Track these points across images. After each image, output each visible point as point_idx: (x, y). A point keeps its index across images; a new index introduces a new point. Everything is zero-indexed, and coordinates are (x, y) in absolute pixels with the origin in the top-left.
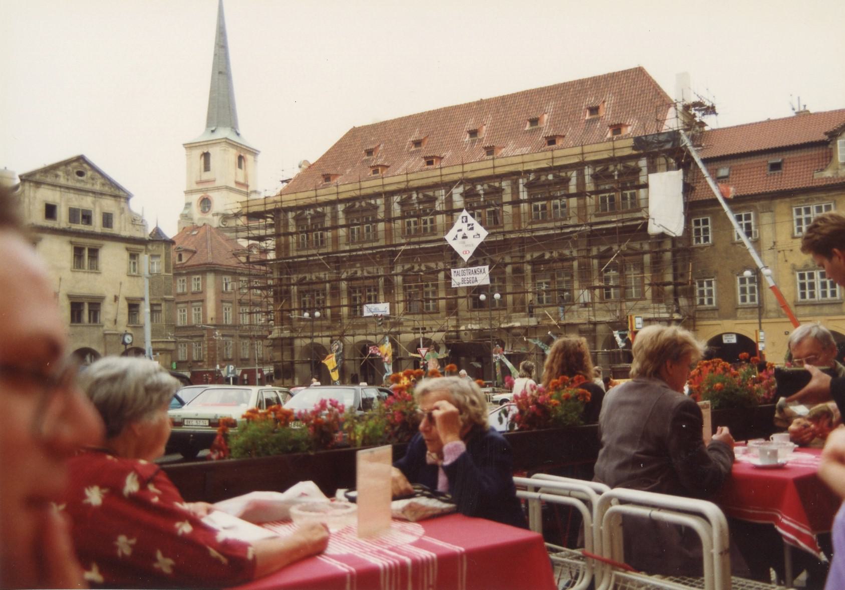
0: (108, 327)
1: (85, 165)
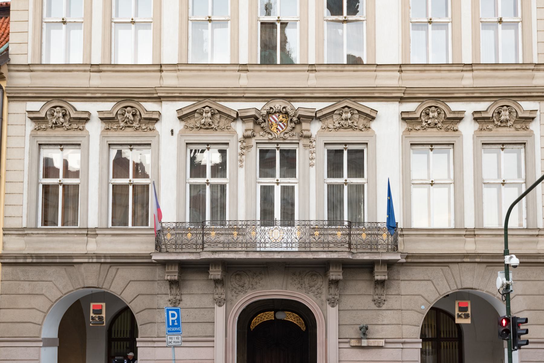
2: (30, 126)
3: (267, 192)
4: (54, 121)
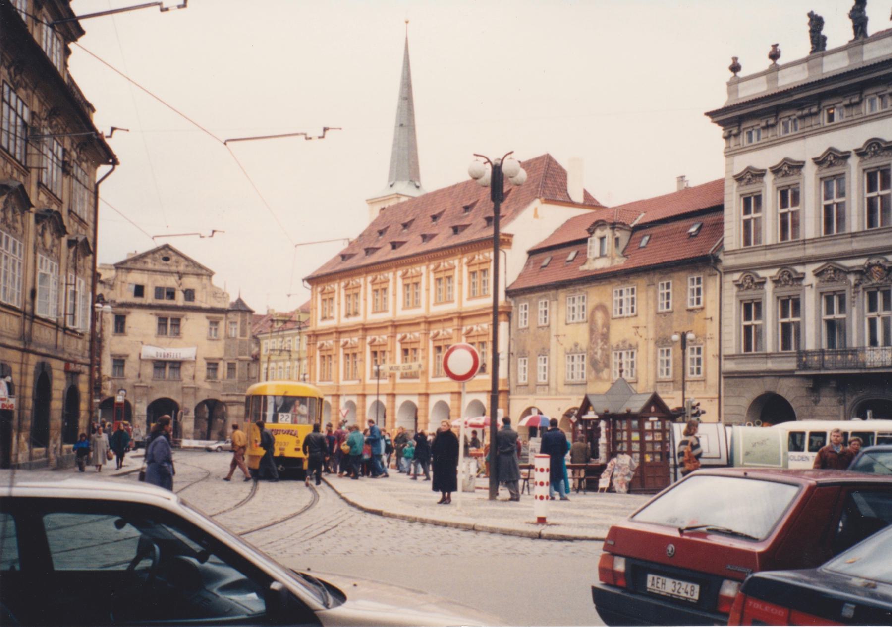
0: (187, 381)
1: (170, 252)
2: (736, 289)
3: (872, 322)
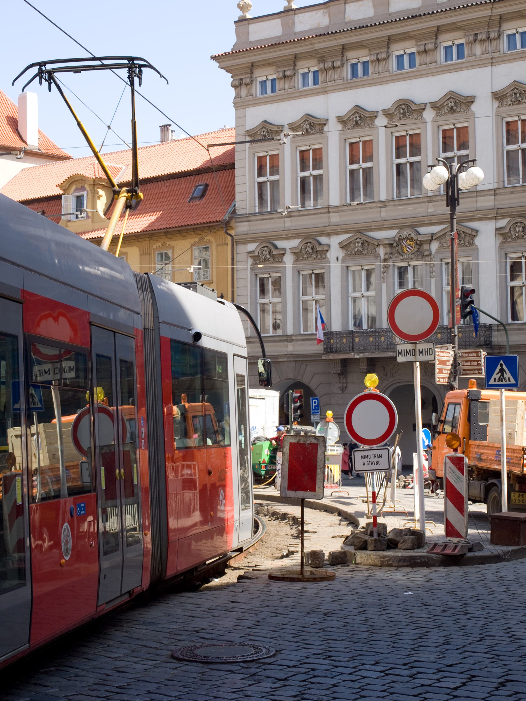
2: (250, 261)
4: (263, 257)
